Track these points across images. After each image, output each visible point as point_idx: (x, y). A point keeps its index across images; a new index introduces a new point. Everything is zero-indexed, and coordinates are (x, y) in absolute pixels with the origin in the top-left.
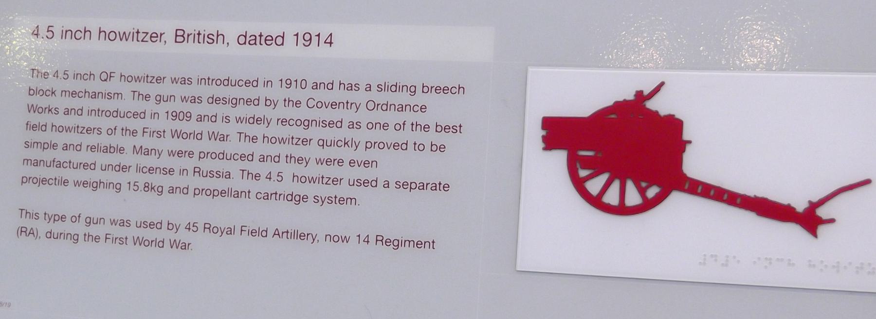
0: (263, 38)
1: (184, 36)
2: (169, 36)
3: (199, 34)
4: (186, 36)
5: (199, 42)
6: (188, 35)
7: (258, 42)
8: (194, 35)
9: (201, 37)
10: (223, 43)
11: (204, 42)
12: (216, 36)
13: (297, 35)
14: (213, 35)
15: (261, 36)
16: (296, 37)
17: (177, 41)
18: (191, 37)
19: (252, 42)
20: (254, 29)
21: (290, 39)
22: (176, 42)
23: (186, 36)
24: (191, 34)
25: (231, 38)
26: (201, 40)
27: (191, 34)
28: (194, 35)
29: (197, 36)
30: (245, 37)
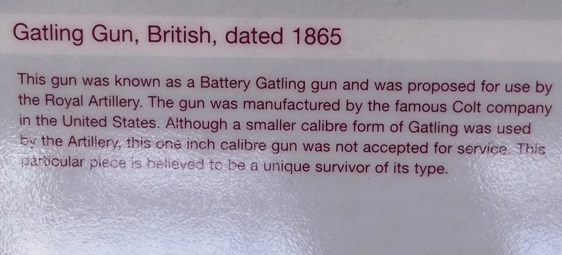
0: (257, 36)
1: (160, 33)
2: (141, 33)
3: (178, 31)
4: (162, 33)
5: (179, 41)
6: (165, 33)
7: (251, 40)
8: (173, 31)
9: (182, 35)
10: (209, 42)
11: (185, 41)
12: (199, 32)
13: (298, 31)
14: (196, 33)
15: (254, 32)
16: (296, 33)
17: (152, 39)
18: (169, 36)
19: (244, 40)
20: (245, 25)
21: (289, 37)
22: (150, 41)
23: (162, 33)
24: (169, 31)
25: (218, 34)
26: (182, 38)
27: (169, 31)
28: (173, 31)
29: (176, 34)
30: (235, 33)
